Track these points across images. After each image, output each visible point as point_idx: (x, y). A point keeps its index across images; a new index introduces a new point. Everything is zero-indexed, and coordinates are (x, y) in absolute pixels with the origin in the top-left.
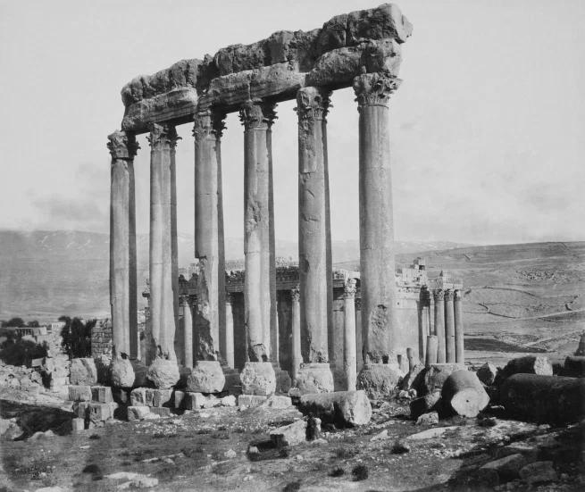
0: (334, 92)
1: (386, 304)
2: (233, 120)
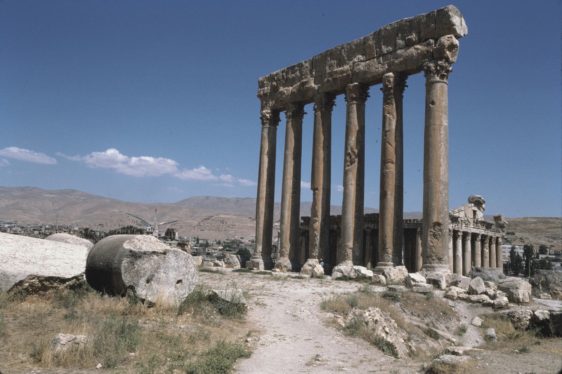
0: (409, 77)
1: (440, 221)
2: (340, 100)
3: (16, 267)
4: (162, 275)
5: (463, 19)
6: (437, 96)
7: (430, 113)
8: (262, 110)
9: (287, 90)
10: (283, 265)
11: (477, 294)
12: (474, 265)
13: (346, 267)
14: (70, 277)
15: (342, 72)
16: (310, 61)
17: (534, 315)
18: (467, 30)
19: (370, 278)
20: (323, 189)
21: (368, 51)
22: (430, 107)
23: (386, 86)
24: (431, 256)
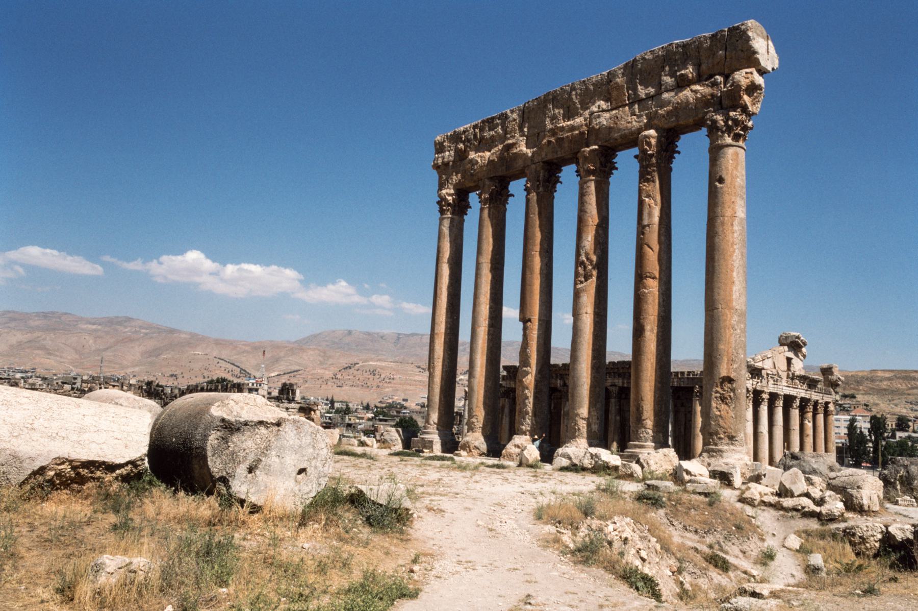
0: (682, 137)
2: (569, 174)
3: (33, 443)
4: (272, 459)
5: (770, 43)
6: (727, 168)
7: (716, 197)
8: (441, 186)
9: (481, 157)
10: (472, 446)
11: (792, 496)
12: (788, 448)
13: (578, 449)
14: (123, 461)
15: (572, 128)
16: (519, 110)
17: (888, 532)
18: (777, 62)
19: (616, 468)
20: (539, 320)
21: (614, 94)
22: (716, 187)
23: (643, 152)
24: (717, 433)
